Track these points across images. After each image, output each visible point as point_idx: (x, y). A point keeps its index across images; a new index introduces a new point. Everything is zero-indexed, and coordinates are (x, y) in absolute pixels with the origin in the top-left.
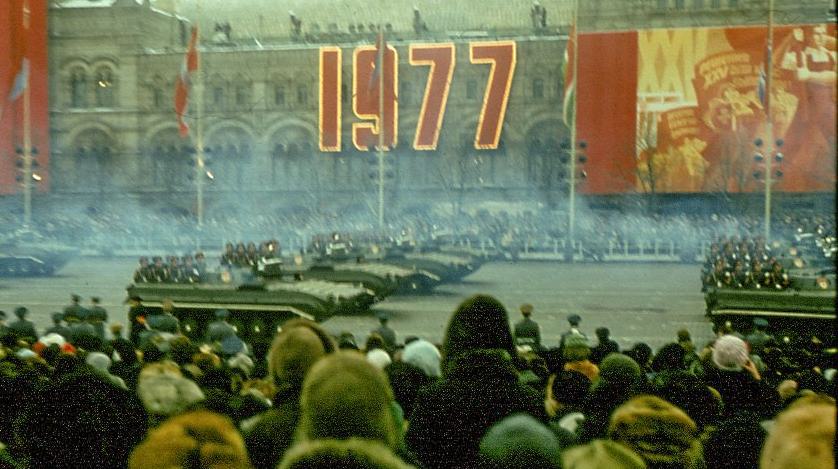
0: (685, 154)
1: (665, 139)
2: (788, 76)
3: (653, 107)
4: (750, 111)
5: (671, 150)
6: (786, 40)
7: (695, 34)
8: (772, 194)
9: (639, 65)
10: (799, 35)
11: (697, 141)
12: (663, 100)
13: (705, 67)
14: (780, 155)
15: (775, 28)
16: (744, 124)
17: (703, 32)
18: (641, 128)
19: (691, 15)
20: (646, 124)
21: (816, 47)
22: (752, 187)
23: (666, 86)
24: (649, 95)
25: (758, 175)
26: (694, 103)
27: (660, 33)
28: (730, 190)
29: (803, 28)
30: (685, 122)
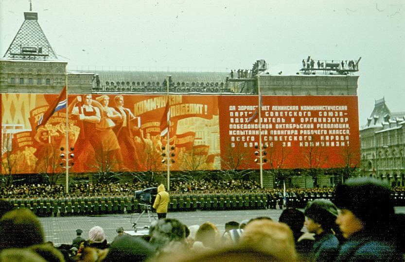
0: (26, 154)
1: (16, 147)
2: (75, 117)
3: (9, 131)
4: (57, 134)
5: (19, 152)
6: (74, 101)
7: (29, 96)
8: (69, 174)
9: (2, 111)
10: (79, 99)
11: (31, 148)
12: (14, 128)
13: (35, 112)
14: (72, 155)
15: (68, 95)
16: (55, 140)
17: (34, 95)
18: (4, 141)
19: (28, 87)
20: (6, 139)
21: (88, 105)
22: (60, 170)
23: (16, 121)
24: (7, 125)
25: (63, 164)
26: (31, 130)
27: (12, 95)
28: (48, 172)
29: (82, 96)
30: (25, 139)
